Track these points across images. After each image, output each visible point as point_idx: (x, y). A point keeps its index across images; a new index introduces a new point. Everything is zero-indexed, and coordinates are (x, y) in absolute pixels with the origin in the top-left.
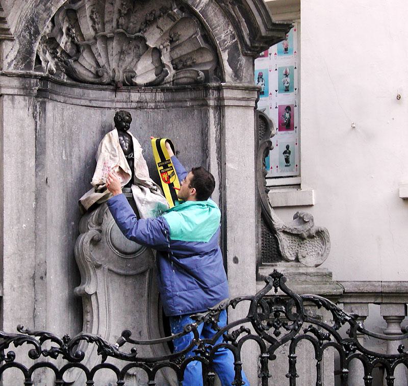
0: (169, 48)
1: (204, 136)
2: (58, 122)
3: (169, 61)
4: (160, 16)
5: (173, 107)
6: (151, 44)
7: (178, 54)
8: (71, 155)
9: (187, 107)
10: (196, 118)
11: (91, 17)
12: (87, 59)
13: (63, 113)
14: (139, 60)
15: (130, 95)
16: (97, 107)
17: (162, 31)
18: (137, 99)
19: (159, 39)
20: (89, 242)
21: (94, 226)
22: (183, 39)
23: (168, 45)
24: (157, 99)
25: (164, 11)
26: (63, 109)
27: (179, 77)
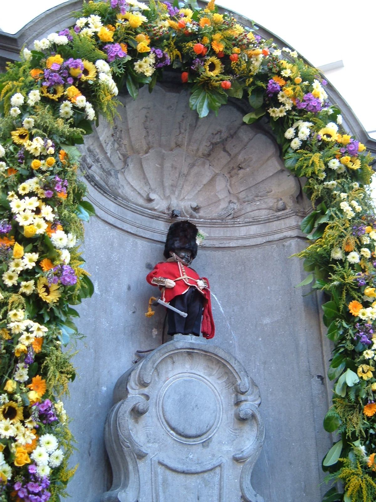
2: (90, 239)
19: (225, 166)
20: (127, 412)
21: (138, 388)
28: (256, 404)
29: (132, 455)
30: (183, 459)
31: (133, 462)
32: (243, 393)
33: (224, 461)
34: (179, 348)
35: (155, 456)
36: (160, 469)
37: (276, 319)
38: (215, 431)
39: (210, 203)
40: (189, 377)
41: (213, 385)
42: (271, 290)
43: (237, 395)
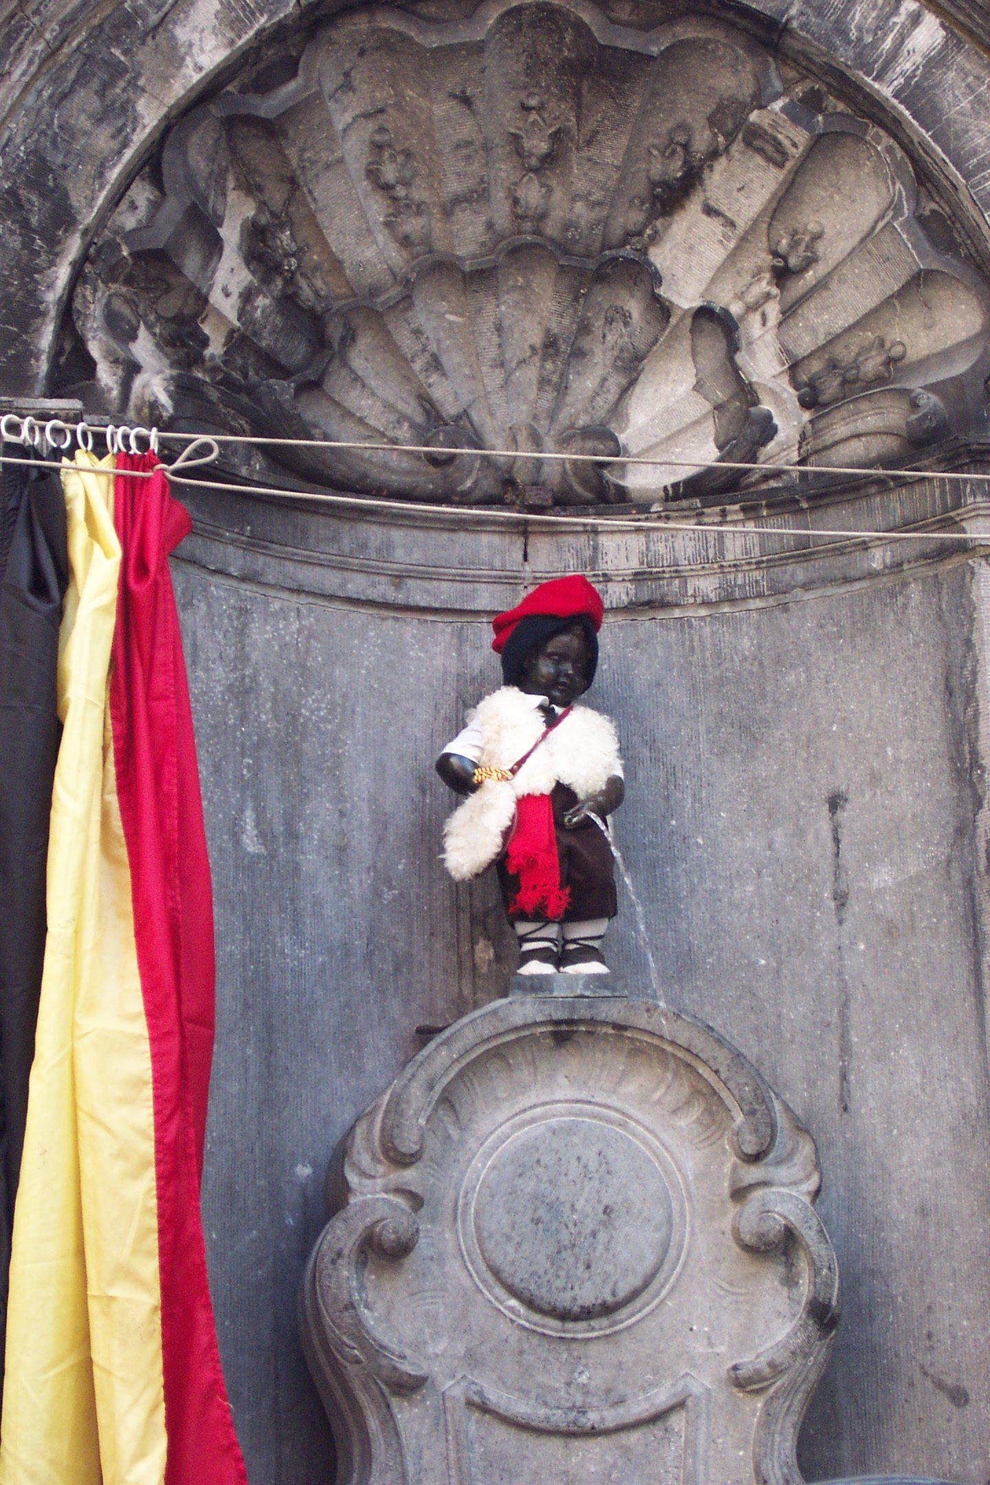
0: (773, 310)
1: (959, 699)
3: (780, 369)
4: (714, 154)
5: (807, 586)
6: (686, 294)
7: (814, 330)
8: (292, 835)
9: (872, 575)
10: (915, 619)
11: (372, 174)
12: (373, 383)
13: (242, 632)
14: (632, 383)
15: (595, 548)
16: (435, 611)
17: (733, 224)
18: (634, 565)
19: (722, 269)
21: (381, 1169)
22: (832, 252)
23: (768, 296)
24: (729, 556)
25: (730, 125)
26: (243, 612)
27: (828, 439)
28: (803, 1194)
29: (373, 1387)
30: (556, 1390)
31: (379, 1408)
32: (755, 1158)
33: (696, 1389)
34: (520, 1022)
35: (458, 1382)
36: (473, 1425)
37: (913, 870)
38: (664, 1292)
39: (675, 428)
40: (570, 1113)
41: (657, 1137)
42: (897, 760)
43: (735, 1168)
